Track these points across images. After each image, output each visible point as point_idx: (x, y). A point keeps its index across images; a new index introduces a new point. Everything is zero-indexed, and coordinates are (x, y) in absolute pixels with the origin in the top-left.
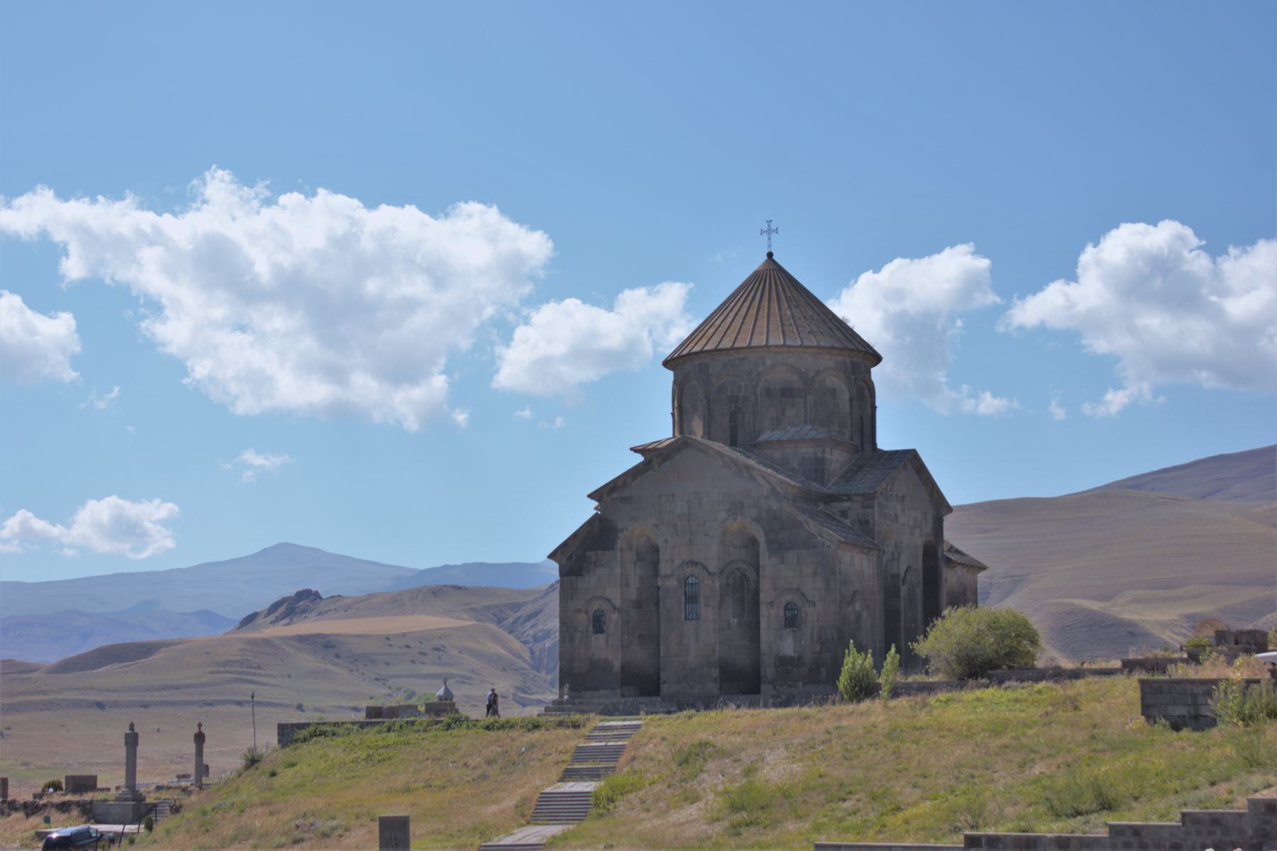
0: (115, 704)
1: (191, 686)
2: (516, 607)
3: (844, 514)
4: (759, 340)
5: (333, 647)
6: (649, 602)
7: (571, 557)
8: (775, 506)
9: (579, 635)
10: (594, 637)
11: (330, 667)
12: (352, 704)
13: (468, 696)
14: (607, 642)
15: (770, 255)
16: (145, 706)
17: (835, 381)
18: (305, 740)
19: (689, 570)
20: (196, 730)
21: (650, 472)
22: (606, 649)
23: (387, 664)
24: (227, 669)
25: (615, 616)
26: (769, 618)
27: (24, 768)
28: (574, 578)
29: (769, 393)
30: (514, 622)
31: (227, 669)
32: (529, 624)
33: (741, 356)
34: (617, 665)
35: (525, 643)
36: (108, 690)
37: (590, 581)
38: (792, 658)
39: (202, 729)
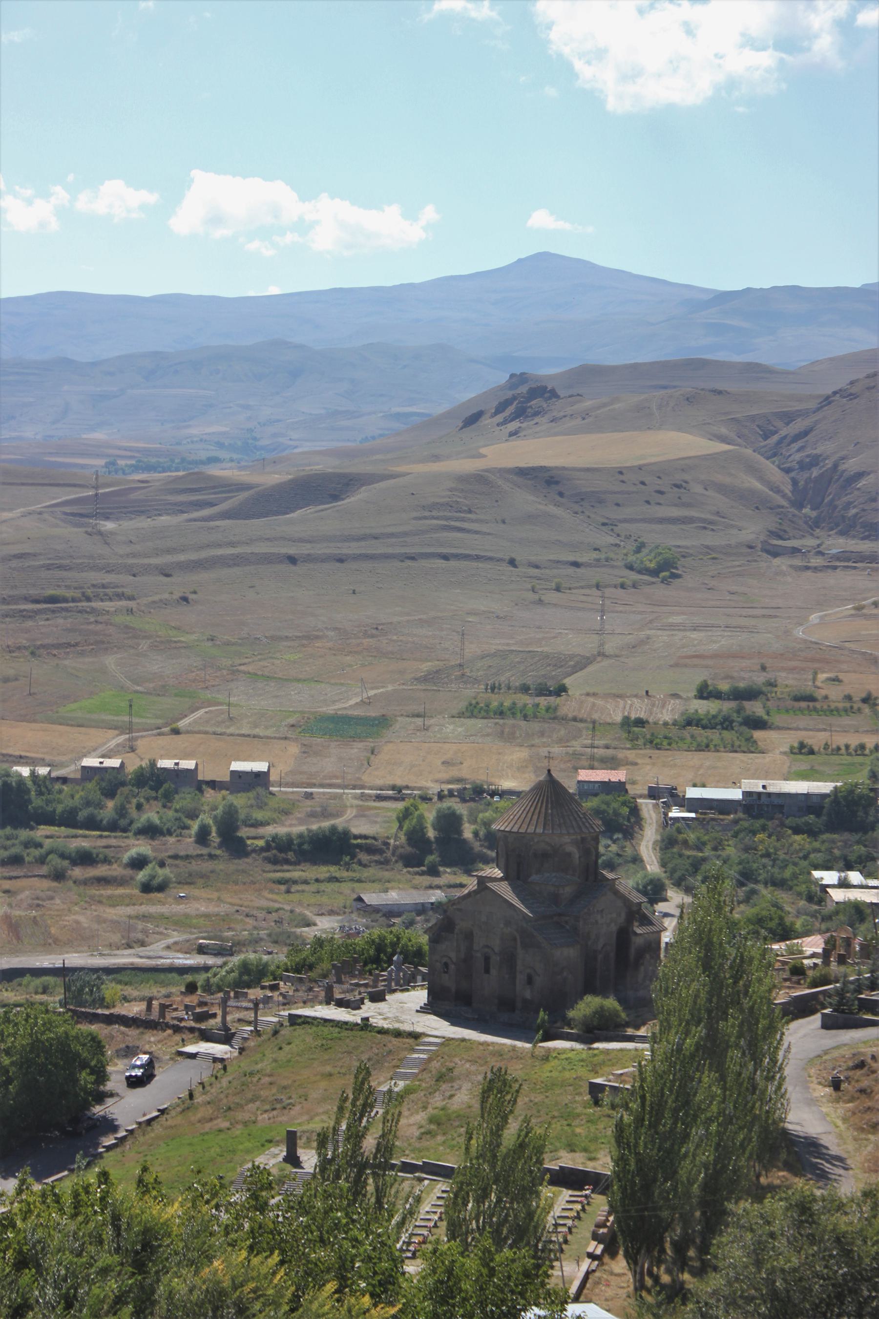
0: (310, 559)
1: (392, 535)
2: (788, 418)
3: (566, 922)
4: (531, 830)
5: (557, 483)
11: (552, 509)
12: (571, 558)
13: (707, 547)
16: (341, 561)
18: (299, 1025)
19: (486, 950)
22: (448, 981)
23: (618, 505)
24: (435, 513)
26: (521, 978)
27: (210, 644)
30: (780, 442)
31: (435, 513)
32: (795, 446)
35: (788, 471)
36: (301, 540)
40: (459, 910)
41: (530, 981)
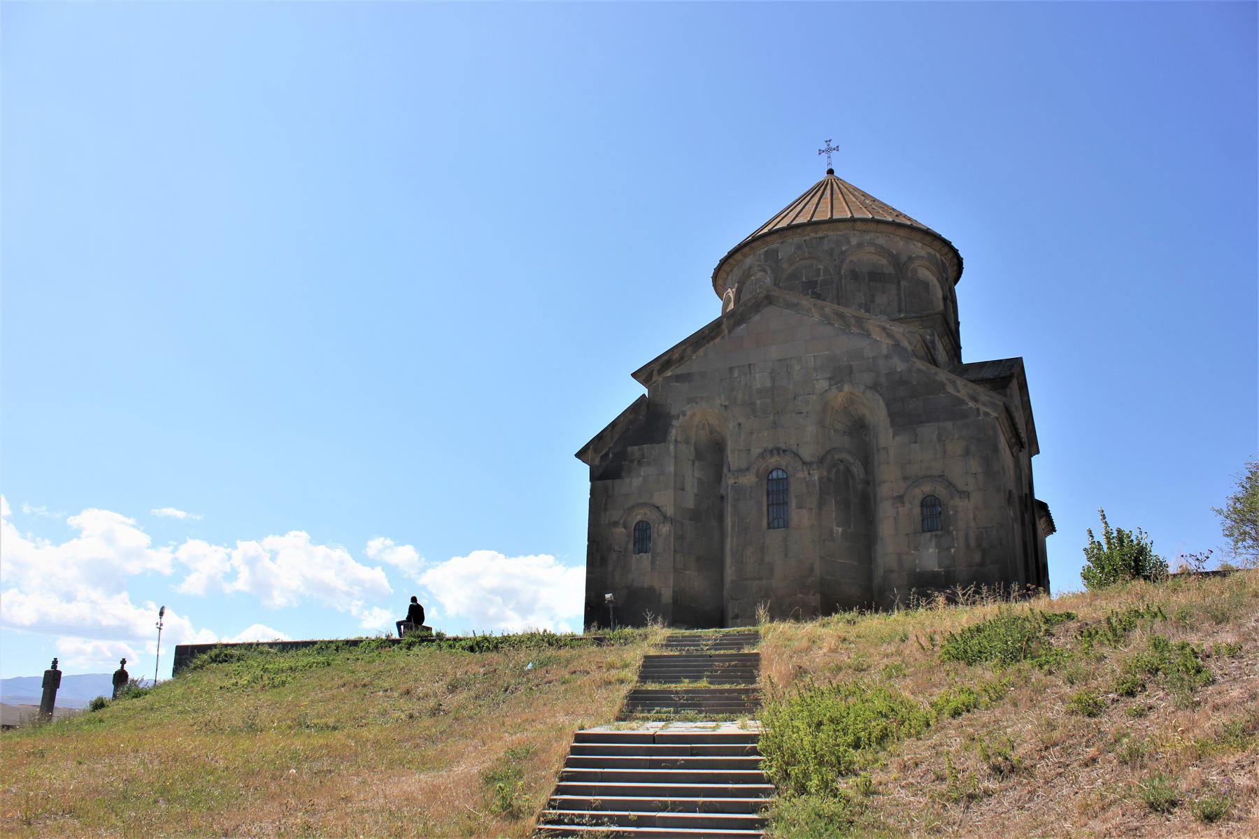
6: (709, 512)
7: (606, 455)
8: (900, 366)
10: (635, 558)
14: (653, 562)
15: (831, 172)
17: (926, 274)
18: (202, 667)
19: (774, 461)
20: (119, 667)
21: (717, 340)
25: (665, 529)
28: (609, 482)
29: (854, 275)
33: (820, 234)
34: (667, 595)
37: (631, 484)
38: (935, 575)
39: (126, 668)
40: (678, 378)
41: (933, 516)
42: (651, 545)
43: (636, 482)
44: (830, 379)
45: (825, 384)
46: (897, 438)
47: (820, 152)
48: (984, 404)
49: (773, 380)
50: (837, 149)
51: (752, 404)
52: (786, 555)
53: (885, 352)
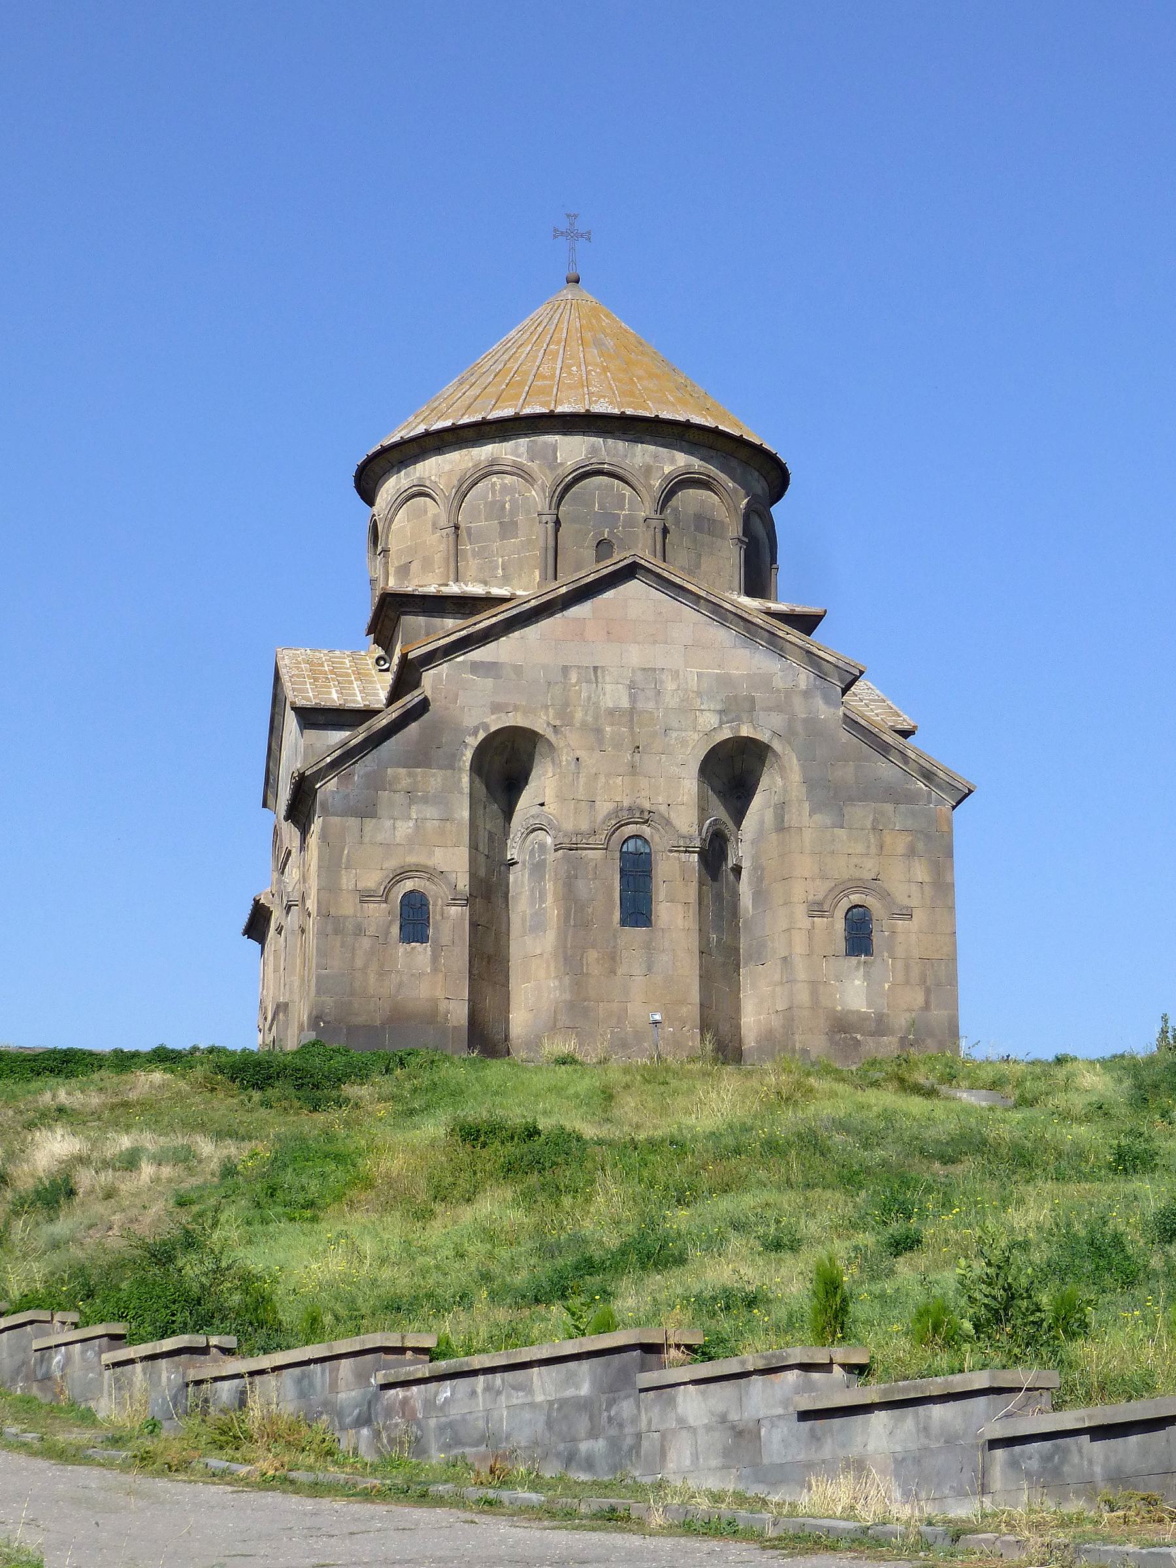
9: (366, 943)
10: (402, 948)
14: (435, 958)
25: (454, 910)
28: (352, 822)
38: (864, 1017)
40: (475, 667)
42: (431, 931)
43: (404, 829)
44: (721, 712)
45: (711, 720)
46: (817, 817)
47: (557, 234)
48: (939, 786)
49: (633, 698)
50: (587, 236)
51: (599, 731)
52: (649, 969)
53: (803, 686)
